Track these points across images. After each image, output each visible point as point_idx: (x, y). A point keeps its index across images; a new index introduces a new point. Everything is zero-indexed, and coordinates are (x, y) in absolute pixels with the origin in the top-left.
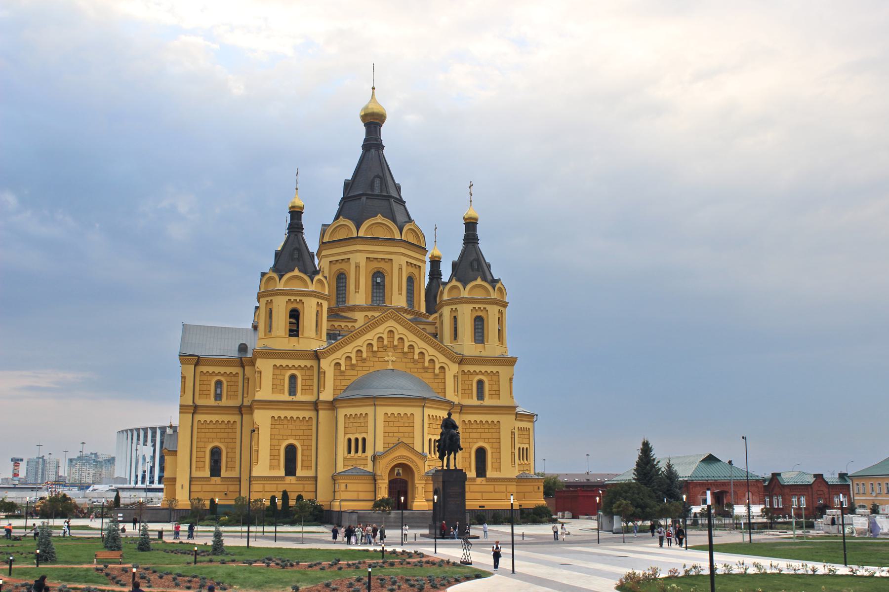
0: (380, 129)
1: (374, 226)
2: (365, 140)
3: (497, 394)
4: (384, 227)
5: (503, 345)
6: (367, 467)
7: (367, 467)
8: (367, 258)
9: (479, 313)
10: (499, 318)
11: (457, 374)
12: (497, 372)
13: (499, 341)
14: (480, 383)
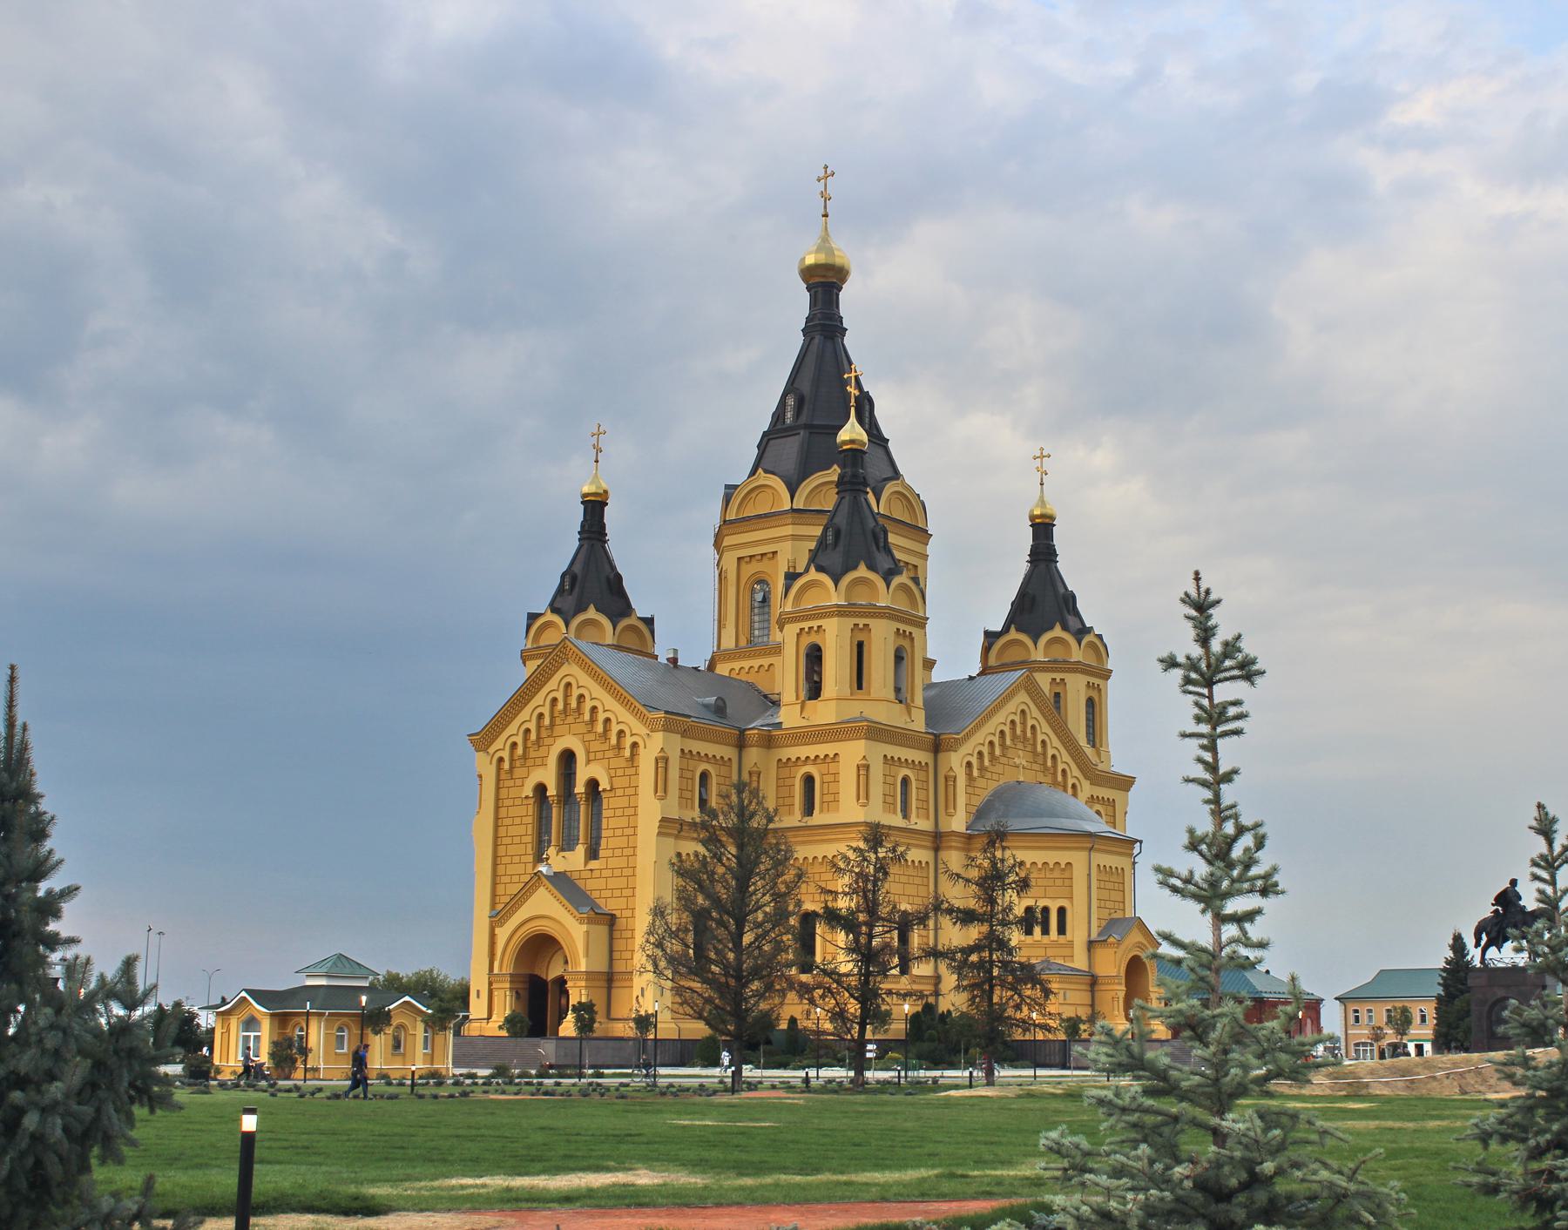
0: (838, 295)
1: (753, 495)
2: (808, 320)
3: (833, 802)
4: (769, 491)
5: (869, 693)
6: (1073, 961)
7: (1073, 961)
8: (739, 559)
9: (814, 638)
10: (860, 645)
11: (864, 762)
12: (836, 754)
13: (860, 687)
14: (809, 781)
